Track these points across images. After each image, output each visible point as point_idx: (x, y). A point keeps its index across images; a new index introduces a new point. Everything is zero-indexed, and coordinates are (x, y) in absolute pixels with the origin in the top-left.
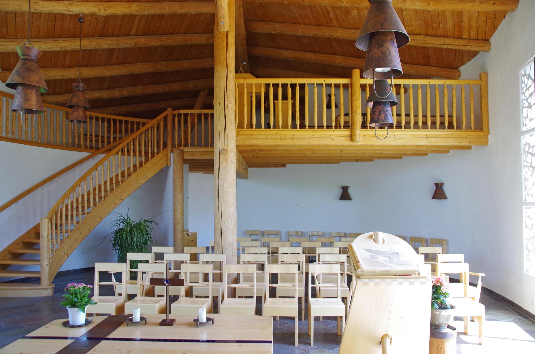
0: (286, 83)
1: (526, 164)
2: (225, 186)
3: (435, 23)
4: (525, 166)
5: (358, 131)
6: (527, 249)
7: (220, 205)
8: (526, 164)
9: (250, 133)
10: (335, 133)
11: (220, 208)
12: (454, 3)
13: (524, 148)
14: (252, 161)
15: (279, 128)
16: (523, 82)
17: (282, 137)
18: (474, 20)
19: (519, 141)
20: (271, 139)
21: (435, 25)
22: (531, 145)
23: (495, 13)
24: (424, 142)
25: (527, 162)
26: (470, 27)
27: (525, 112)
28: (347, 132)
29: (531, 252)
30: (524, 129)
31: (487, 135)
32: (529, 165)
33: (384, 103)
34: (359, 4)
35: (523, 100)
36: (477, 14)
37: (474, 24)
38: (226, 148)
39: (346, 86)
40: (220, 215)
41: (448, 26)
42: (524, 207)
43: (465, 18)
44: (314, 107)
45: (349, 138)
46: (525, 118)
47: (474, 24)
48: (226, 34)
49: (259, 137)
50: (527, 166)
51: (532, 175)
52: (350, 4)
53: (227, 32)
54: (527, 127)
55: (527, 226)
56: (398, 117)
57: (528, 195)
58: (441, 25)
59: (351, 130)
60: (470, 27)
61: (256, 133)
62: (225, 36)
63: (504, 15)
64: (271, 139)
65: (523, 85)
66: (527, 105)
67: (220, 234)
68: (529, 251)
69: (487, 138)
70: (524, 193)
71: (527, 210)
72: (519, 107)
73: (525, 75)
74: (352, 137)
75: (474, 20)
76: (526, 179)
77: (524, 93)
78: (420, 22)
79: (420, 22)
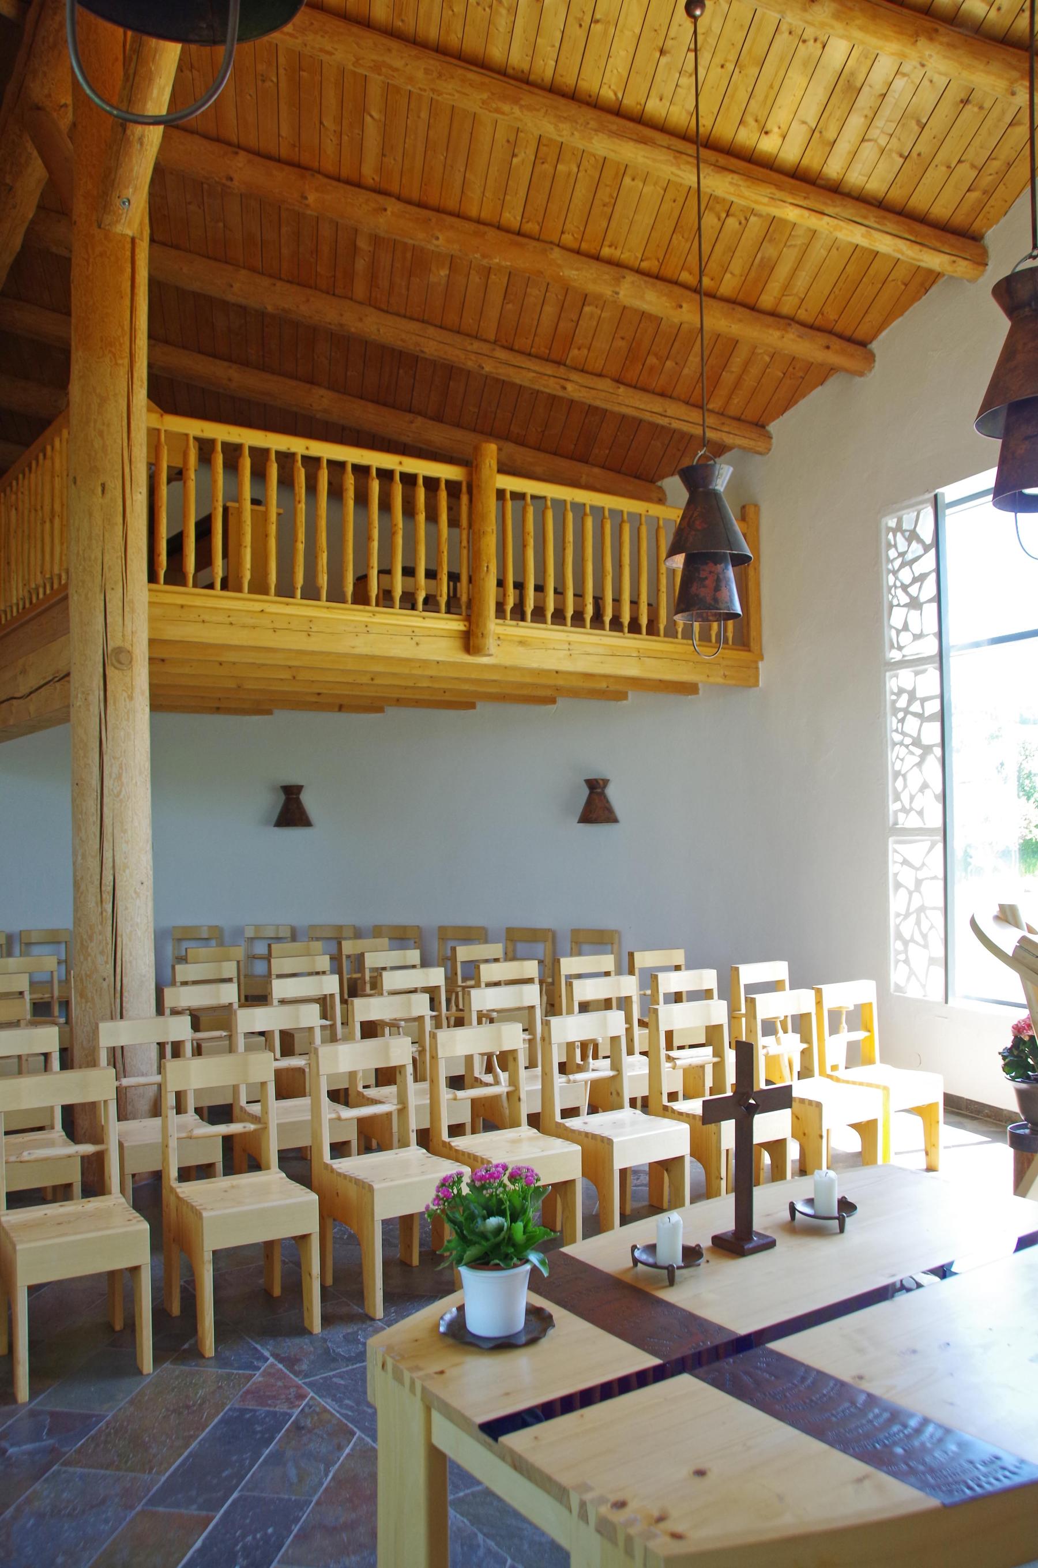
0: (293, 450)
1: (897, 737)
2: (124, 780)
3: (656, 355)
4: (895, 744)
5: (494, 627)
6: (899, 936)
7: (107, 845)
8: (897, 737)
9: (180, 600)
10: (379, 619)
11: (108, 855)
12: (740, 321)
13: (894, 702)
14: (187, 693)
15: (240, 590)
16: (889, 546)
17: (277, 625)
18: (754, 371)
19: (881, 684)
20: (244, 626)
21: (652, 360)
22: (919, 695)
23: (809, 366)
24: (632, 669)
25: (903, 733)
26: (737, 384)
27: (897, 617)
28: (456, 625)
29: (911, 945)
30: (895, 655)
31: (756, 662)
32: (908, 741)
33: (717, 559)
34: (484, 256)
35: (890, 588)
36: (767, 359)
37: (749, 381)
38: (128, 646)
39: (453, 488)
40: (108, 879)
41: (686, 371)
42: (891, 840)
43: (737, 362)
44: (369, 538)
45: (458, 643)
46: (898, 632)
47: (749, 381)
48: (128, 246)
49: (206, 618)
50: (901, 744)
51: (919, 765)
52: (456, 246)
53: (133, 240)
54: (905, 651)
55: (898, 886)
56: (539, 594)
57: (906, 811)
58: (669, 364)
59: (468, 619)
60: (737, 384)
61: (198, 602)
62: (128, 254)
63: (823, 374)
64: (244, 626)
65: (893, 554)
66: (904, 599)
67: (110, 948)
68: (906, 943)
69: (757, 668)
70: (894, 807)
71: (898, 847)
72: (881, 603)
73: (899, 528)
74: (470, 641)
75: (754, 371)
76: (897, 774)
77: (895, 573)
78: (619, 343)
79: (619, 343)
